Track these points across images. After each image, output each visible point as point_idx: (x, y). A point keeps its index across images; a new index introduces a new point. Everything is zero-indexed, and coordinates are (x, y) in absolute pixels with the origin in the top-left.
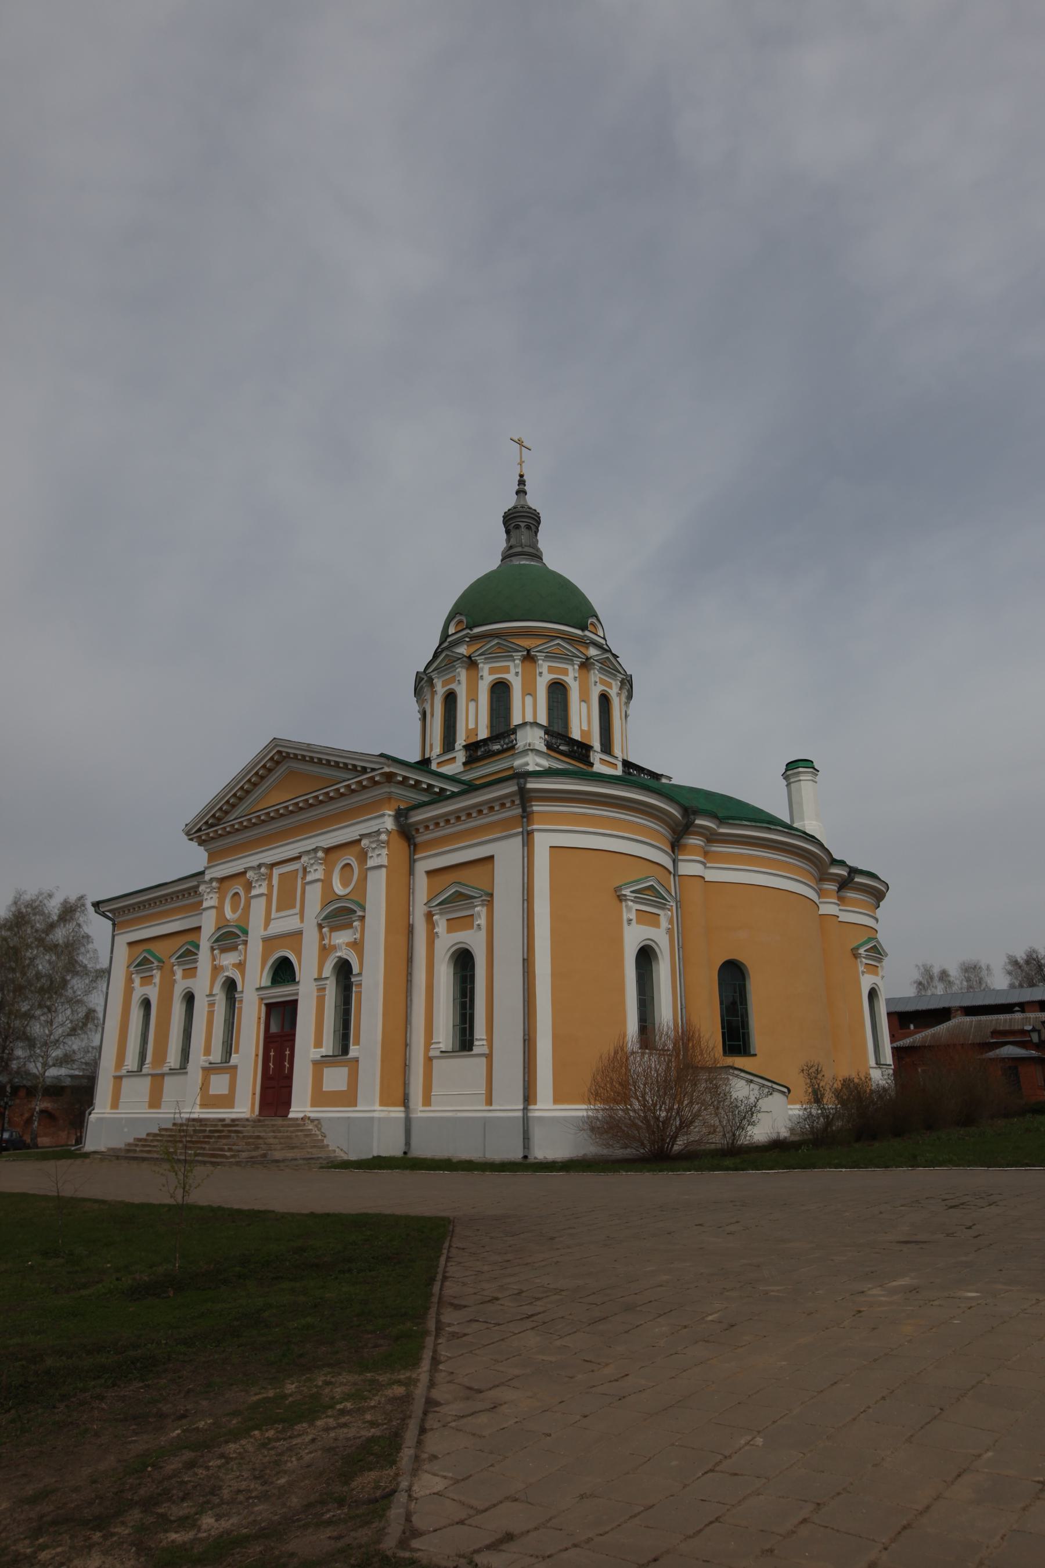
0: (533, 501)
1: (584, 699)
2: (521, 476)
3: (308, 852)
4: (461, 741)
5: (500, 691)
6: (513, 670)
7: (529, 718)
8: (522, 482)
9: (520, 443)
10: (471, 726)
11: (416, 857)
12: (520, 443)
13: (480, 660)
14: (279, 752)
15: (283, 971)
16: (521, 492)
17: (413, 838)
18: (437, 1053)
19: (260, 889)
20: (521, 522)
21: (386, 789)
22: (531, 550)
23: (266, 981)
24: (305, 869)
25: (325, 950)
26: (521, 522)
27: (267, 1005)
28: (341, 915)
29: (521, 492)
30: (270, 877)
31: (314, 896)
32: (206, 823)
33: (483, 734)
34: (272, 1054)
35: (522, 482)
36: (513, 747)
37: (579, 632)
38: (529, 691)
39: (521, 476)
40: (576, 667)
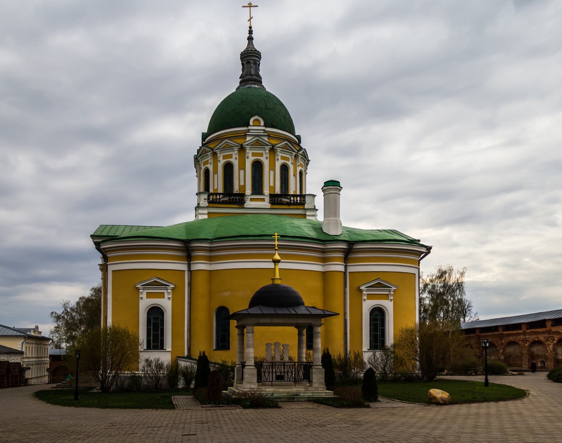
0: (257, 45)
2: (250, 28)
4: (266, 191)
5: (284, 169)
8: (251, 32)
9: (250, 6)
11: (348, 264)
16: (250, 39)
20: (250, 58)
22: (255, 77)
26: (250, 58)
29: (250, 39)
33: (278, 191)
35: (251, 32)
39: (250, 28)
40: (267, 151)
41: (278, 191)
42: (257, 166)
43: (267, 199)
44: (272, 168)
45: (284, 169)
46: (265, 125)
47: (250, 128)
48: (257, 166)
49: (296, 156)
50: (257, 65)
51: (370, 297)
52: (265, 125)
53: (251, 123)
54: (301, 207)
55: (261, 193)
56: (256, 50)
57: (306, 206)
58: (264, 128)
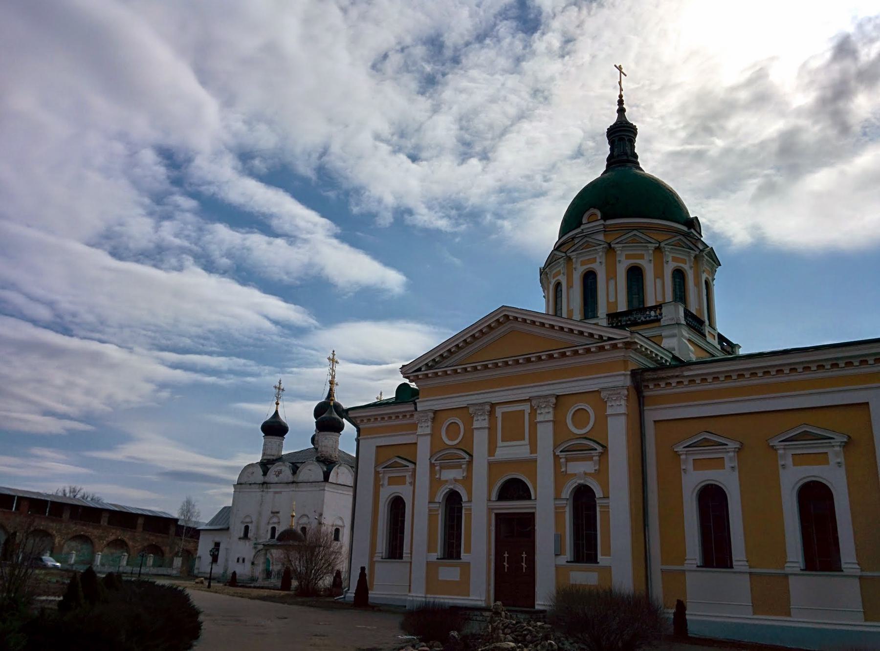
1: (697, 284)
3: (539, 397)
4: (602, 311)
5: (635, 275)
6: (646, 257)
7: (660, 299)
8: (621, 102)
10: (612, 300)
12: (620, 68)
13: (618, 247)
14: (507, 317)
15: (514, 489)
16: (621, 111)
17: (642, 392)
18: (694, 567)
19: (480, 422)
20: (622, 135)
21: (619, 354)
23: (494, 497)
24: (533, 411)
25: (560, 477)
26: (622, 135)
27: (497, 515)
28: (569, 449)
29: (621, 111)
30: (492, 413)
31: (545, 434)
32: (427, 364)
33: (622, 307)
34: (506, 555)
35: (621, 102)
36: (659, 320)
37: (685, 229)
38: (659, 275)
41: (622, 307)
42: (590, 279)
43: (604, 322)
44: (612, 275)
45: (635, 275)
46: (605, 217)
47: (582, 227)
48: (590, 279)
49: (658, 249)
50: (632, 142)
51: (699, 464)
52: (605, 217)
53: (584, 221)
54: (656, 324)
55: (595, 316)
56: (627, 123)
57: (662, 323)
58: (602, 222)
